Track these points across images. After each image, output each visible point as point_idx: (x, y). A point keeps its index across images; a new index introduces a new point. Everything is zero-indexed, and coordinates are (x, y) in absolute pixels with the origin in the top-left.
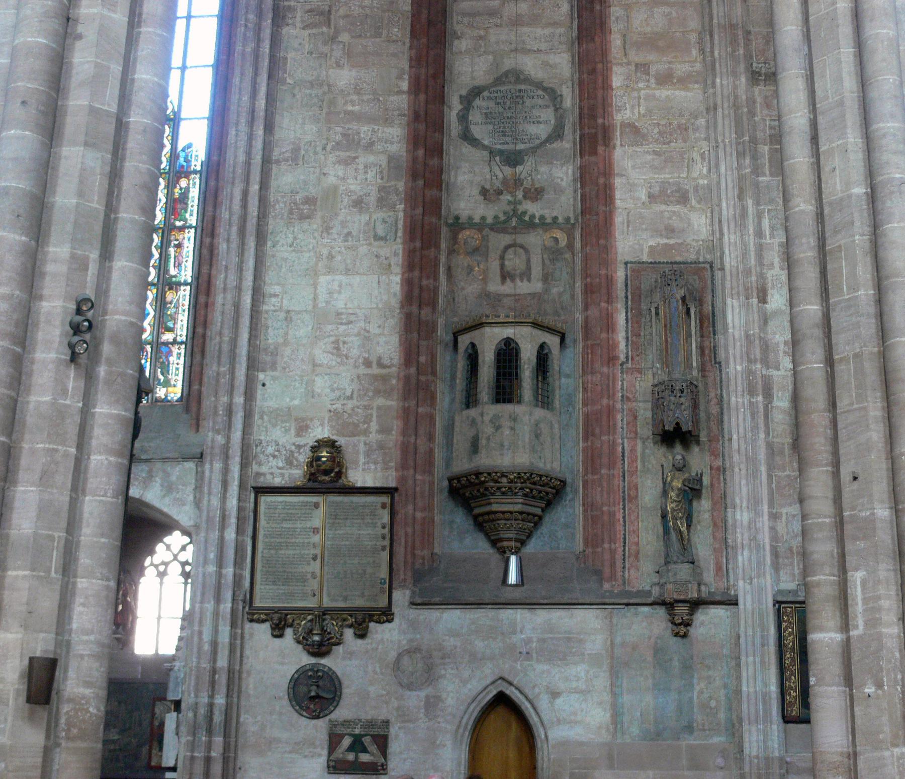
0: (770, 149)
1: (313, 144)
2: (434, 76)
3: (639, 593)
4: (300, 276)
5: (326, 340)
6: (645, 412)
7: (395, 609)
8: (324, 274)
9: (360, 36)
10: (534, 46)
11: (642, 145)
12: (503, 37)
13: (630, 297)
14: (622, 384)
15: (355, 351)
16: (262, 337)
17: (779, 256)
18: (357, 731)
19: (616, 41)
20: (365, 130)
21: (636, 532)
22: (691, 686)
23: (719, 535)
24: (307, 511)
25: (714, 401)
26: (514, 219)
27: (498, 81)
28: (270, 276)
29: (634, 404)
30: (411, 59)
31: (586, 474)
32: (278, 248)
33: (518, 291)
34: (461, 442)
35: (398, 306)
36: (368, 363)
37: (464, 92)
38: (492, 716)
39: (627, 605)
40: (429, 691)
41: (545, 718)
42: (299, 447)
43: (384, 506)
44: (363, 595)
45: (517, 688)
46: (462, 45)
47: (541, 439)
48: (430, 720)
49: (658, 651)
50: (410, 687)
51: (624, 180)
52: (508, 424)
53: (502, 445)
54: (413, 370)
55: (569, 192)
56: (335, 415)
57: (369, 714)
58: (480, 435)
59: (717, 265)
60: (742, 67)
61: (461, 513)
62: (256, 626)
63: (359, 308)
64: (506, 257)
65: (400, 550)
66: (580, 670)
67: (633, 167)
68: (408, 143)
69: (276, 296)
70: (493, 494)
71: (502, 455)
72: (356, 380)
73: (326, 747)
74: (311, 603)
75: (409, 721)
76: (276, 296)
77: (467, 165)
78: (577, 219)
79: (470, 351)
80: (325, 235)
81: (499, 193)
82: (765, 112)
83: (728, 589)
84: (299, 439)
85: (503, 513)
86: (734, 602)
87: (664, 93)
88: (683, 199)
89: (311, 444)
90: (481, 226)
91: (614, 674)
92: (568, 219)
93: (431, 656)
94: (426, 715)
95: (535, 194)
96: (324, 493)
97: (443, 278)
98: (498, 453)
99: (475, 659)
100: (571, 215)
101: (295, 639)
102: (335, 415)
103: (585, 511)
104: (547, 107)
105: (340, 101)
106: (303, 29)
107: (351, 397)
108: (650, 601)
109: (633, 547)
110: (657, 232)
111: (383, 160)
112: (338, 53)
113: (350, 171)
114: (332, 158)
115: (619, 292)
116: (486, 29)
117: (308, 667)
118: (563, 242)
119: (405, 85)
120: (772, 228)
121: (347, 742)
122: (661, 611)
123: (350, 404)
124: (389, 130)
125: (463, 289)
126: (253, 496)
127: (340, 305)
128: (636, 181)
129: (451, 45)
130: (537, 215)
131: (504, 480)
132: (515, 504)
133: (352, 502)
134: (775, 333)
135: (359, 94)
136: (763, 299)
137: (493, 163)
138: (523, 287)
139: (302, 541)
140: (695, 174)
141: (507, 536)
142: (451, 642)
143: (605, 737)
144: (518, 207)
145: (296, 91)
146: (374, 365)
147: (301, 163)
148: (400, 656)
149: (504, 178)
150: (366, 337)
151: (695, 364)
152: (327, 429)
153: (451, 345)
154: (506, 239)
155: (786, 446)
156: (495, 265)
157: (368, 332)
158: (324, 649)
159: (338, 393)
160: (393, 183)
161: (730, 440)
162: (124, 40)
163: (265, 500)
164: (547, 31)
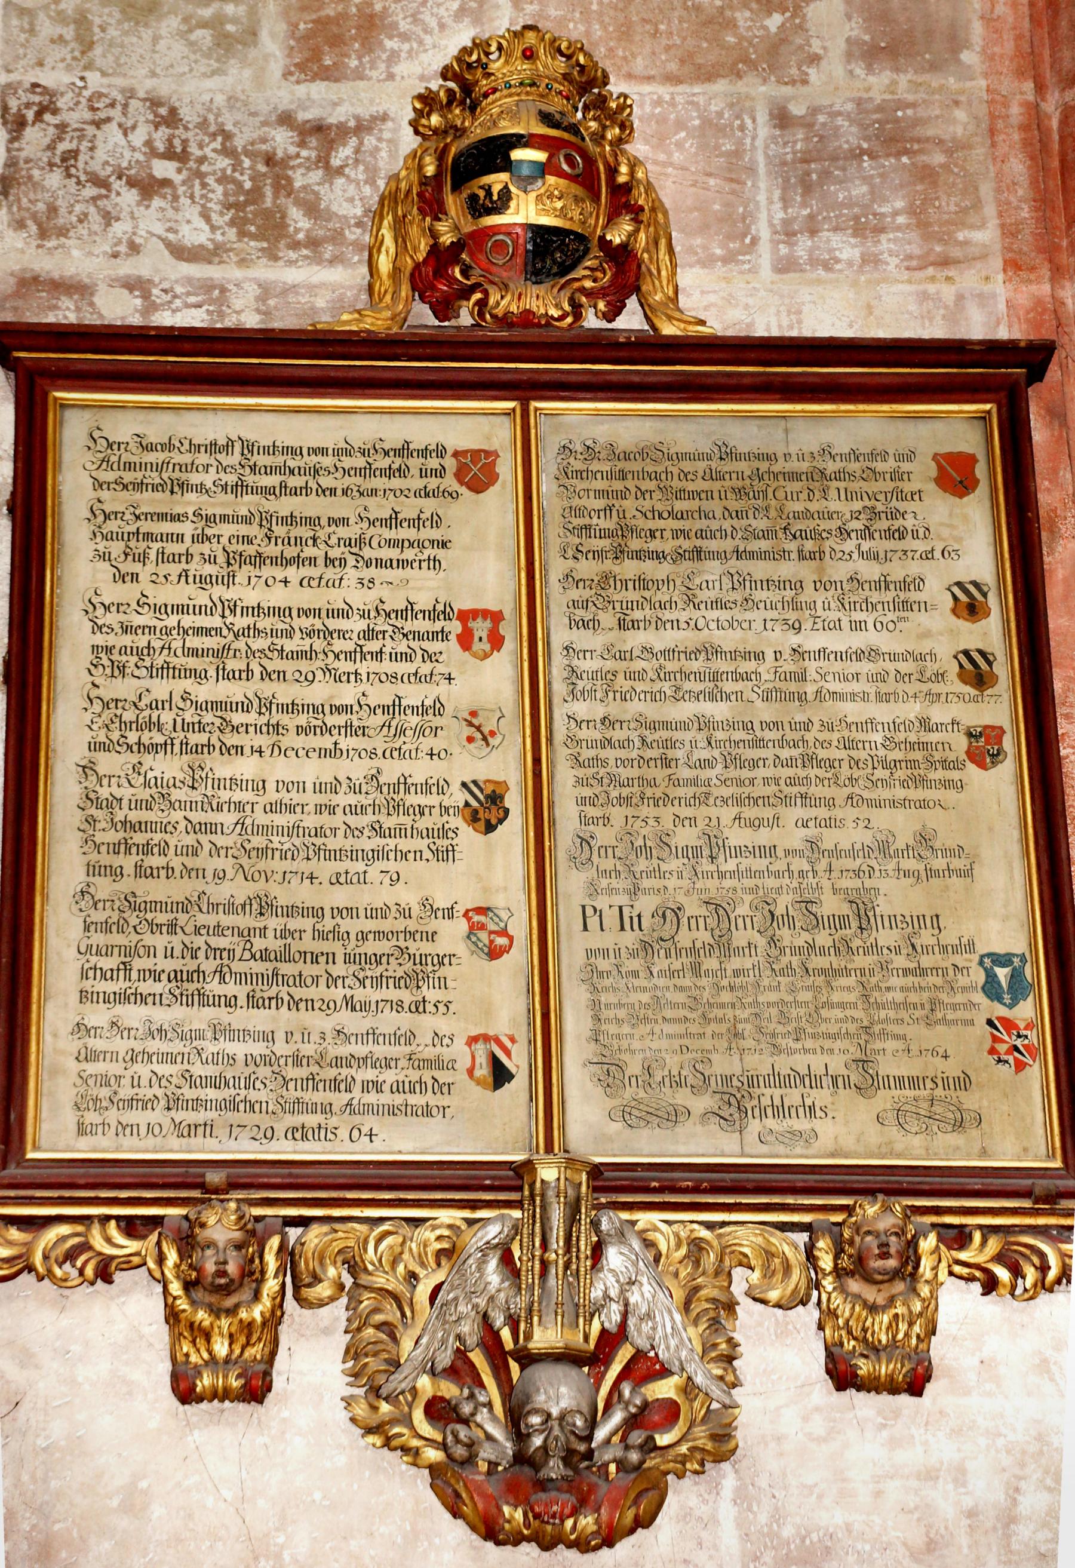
84: (318, 90)
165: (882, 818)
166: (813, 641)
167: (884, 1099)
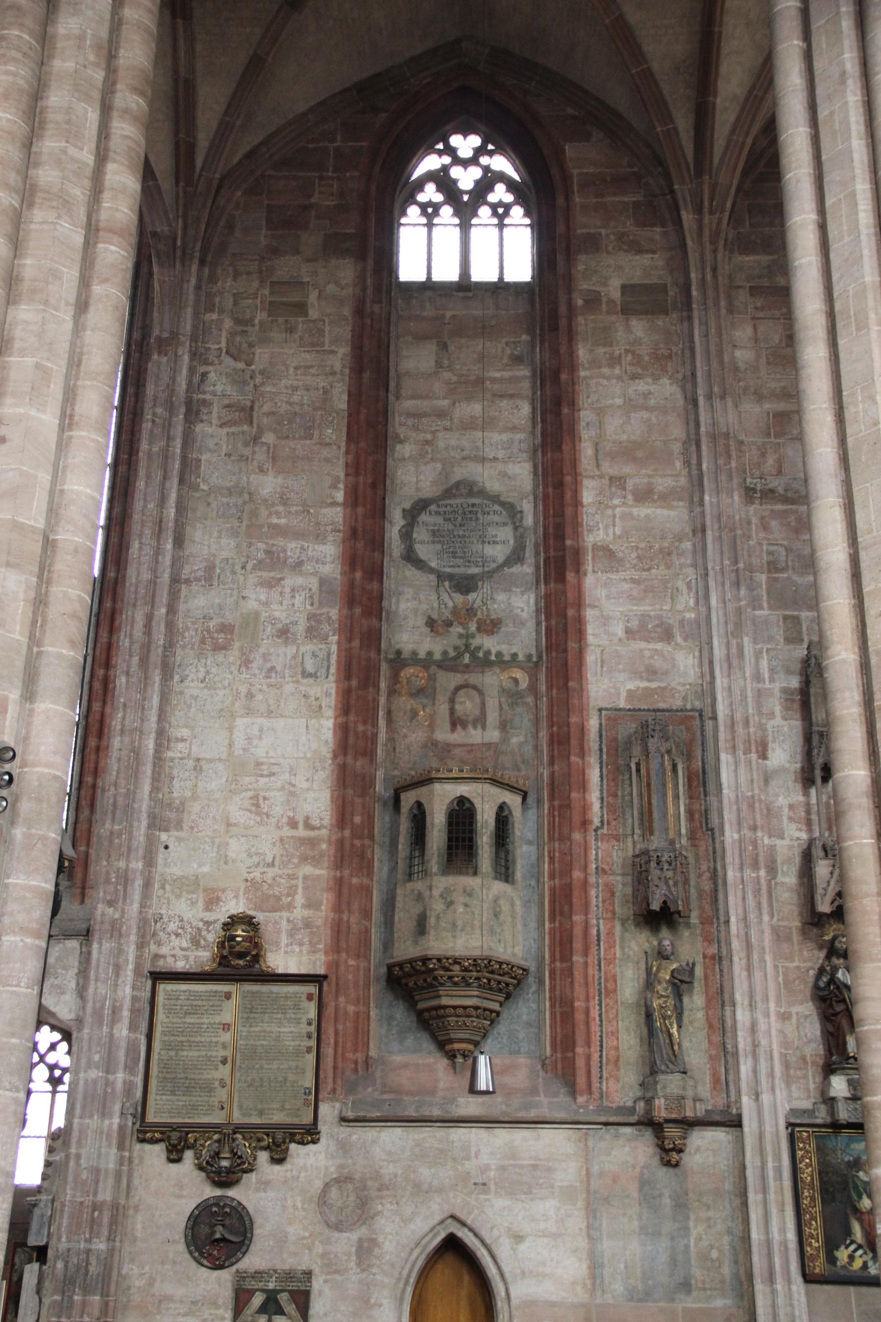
0: (768, 578)
1: (230, 561)
2: (374, 486)
3: (621, 1110)
4: (212, 717)
5: (243, 795)
6: (622, 885)
7: (322, 1127)
8: (242, 716)
9: (287, 437)
10: (490, 453)
11: (617, 571)
12: (453, 442)
13: (605, 750)
14: (597, 854)
15: (278, 808)
16: (166, 790)
17: (780, 704)
18: (271, 1286)
19: (586, 451)
20: (292, 548)
21: (615, 1034)
22: (686, 1229)
23: (716, 1038)
24: (216, 1003)
25: (707, 875)
26: (467, 656)
27: (448, 493)
28: (177, 717)
29: (611, 877)
30: (347, 465)
31: (553, 960)
32: (186, 683)
33: (471, 741)
34: (404, 921)
35: (330, 755)
36: (293, 824)
37: (407, 505)
38: (439, 1266)
39: (606, 1124)
40: (362, 1232)
41: (506, 1269)
42: (208, 923)
43: (310, 997)
44: (282, 1109)
45: (471, 1230)
46: (406, 450)
47: (502, 918)
48: (363, 1270)
49: (644, 1183)
50: (338, 1227)
51: (597, 612)
52: (462, 900)
53: (454, 925)
54: (347, 833)
55: (531, 624)
56: (253, 885)
57: (288, 1262)
58: (428, 914)
59: (708, 713)
60: (735, 481)
61: (402, 1007)
62: (148, 1147)
63: (283, 757)
64: (457, 700)
65: (328, 1051)
66: (549, 1207)
67: (608, 597)
68: (343, 564)
69: (183, 740)
70: (442, 985)
71: (454, 937)
72: (278, 844)
73: (230, 1305)
74: (217, 1118)
75: (337, 1272)
76: (183, 740)
77: (410, 590)
78: (540, 657)
79: (415, 811)
80: (244, 669)
81: (449, 624)
82: (762, 535)
83: (729, 1107)
84: (208, 914)
85: (455, 1007)
86: (736, 1123)
87: (643, 511)
88: (667, 636)
89: (223, 921)
90: (427, 663)
91: (591, 1212)
92: (529, 657)
93: (365, 1188)
94: (358, 1264)
95: (491, 626)
96: (237, 981)
97: (382, 722)
98: (450, 935)
99: (420, 1190)
100: (533, 652)
101: (196, 1165)
102: (253, 885)
103: (553, 1006)
104: (505, 524)
105: (263, 512)
106: (222, 426)
107: (272, 865)
108: (634, 1119)
109: (613, 1053)
110: (636, 674)
111: (314, 583)
112: (261, 455)
113: (275, 595)
114: (252, 579)
115: (592, 744)
116: (433, 433)
117: (212, 1201)
118: (524, 684)
119: (340, 496)
120: (772, 670)
121: (258, 1300)
122: (648, 1135)
123: (271, 872)
124: (321, 548)
125: (405, 736)
126: (149, 983)
127: (260, 753)
128: (611, 614)
129: (393, 450)
130: (494, 651)
131: (457, 968)
132: (470, 999)
133: (271, 993)
134: (777, 795)
135: (285, 504)
136: (764, 756)
137: (442, 589)
138: (475, 736)
139: (208, 1040)
140: (679, 607)
141: (461, 1035)
142: (389, 1170)
143: (581, 1295)
144: (471, 641)
145: (211, 500)
146: (301, 826)
147: (216, 583)
148: (327, 1186)
149: (455, 607)
150: (291, 793)
151: (683, 831)
152: (242, 901)
153: (392, 802)
154: (457, 679)
155: (794, 931)
156: (443, 709)
157: (294, 786)
158: (235, 1177)
159: (256, 859)
160: (325, 610)
161: (727, 922)
162: (53, 446)
163: (165, 989)
164: (505, 437)
165: (290, 1063)
166: (283, 1030)
167: (285, 1112)
